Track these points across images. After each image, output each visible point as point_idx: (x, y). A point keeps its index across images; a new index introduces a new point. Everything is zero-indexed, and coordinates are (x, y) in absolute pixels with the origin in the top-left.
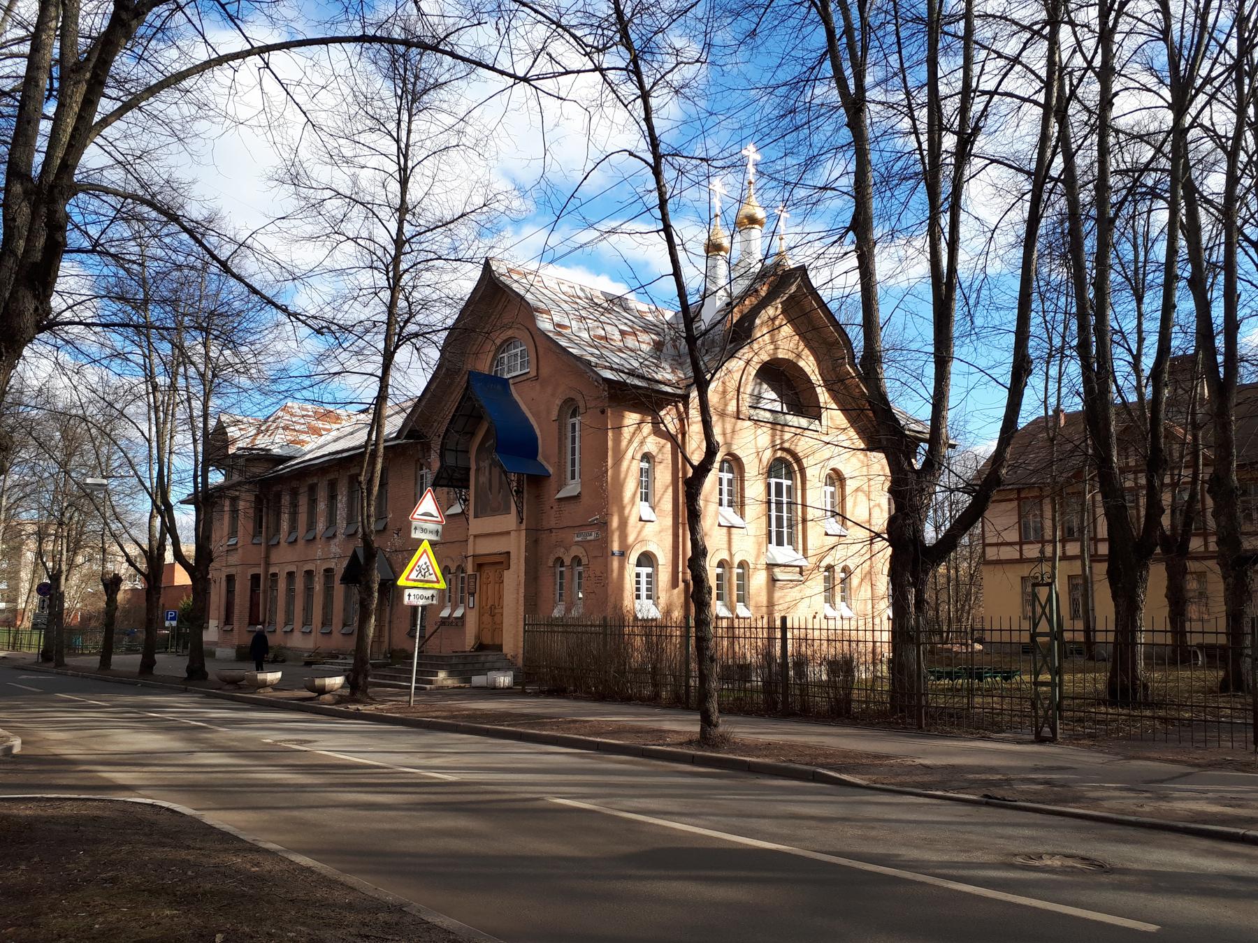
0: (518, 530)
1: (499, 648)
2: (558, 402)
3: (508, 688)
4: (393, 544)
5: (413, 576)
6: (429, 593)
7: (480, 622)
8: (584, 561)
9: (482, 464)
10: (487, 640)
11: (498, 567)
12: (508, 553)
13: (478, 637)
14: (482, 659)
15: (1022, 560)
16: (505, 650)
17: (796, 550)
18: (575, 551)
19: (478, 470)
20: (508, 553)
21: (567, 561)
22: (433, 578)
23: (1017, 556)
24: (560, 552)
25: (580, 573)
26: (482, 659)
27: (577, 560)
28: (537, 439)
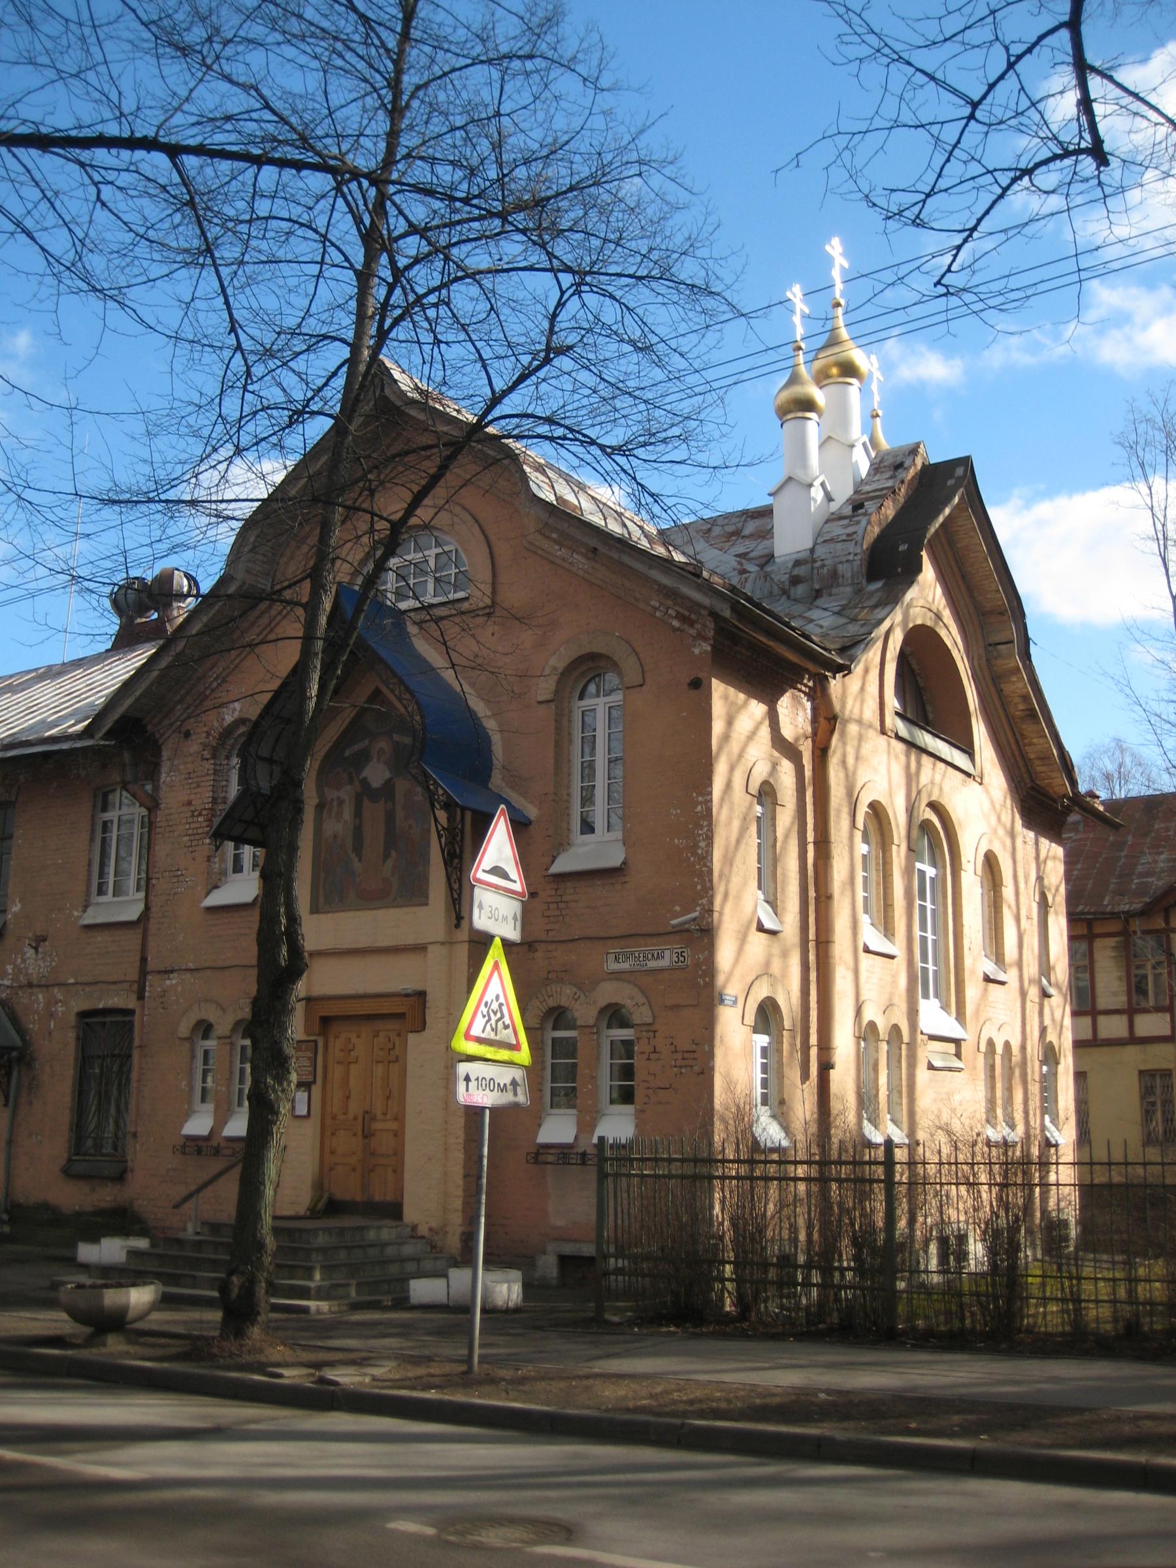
0: (449, 943)
1: (394, 1211)
2: (558, 661)
3: (517, 1310)
4: (18, 970)
5: (476, 1031)
6: (505, 1076)
7: (325, 1151)
8: (641, 1015)
9: (331, 794)
10: (348, 1189)
11: (391, 1025)
12: (422, 995)
13: (319, 1185)
14: (372, 1235)
15: (1133, 1040)
16: (411, 1213)
17: (945, 1007)
18: (608, 993)
19: (320, 807)
20: (422, 995)
21: (585, 1012)
22: (506, 1035)
23: (1123, 1032)
24: (564, 995)
25: (206, 1053)
26: (372, 1235)
27: (615, 1015)
28: (488, 740)
